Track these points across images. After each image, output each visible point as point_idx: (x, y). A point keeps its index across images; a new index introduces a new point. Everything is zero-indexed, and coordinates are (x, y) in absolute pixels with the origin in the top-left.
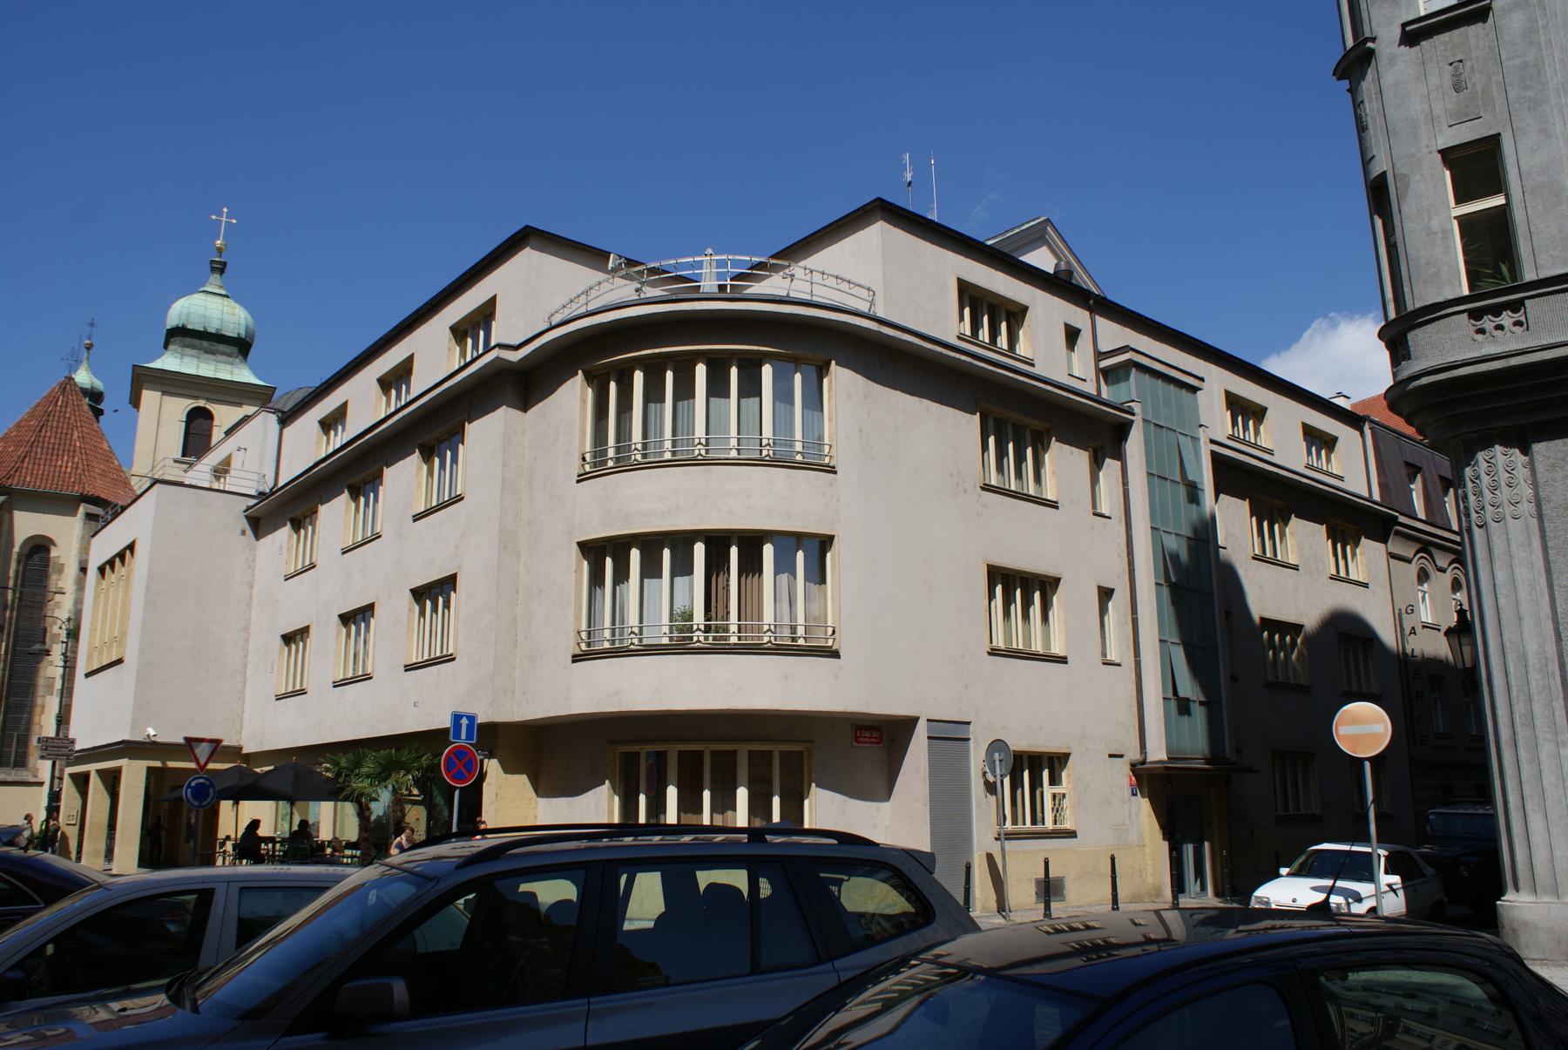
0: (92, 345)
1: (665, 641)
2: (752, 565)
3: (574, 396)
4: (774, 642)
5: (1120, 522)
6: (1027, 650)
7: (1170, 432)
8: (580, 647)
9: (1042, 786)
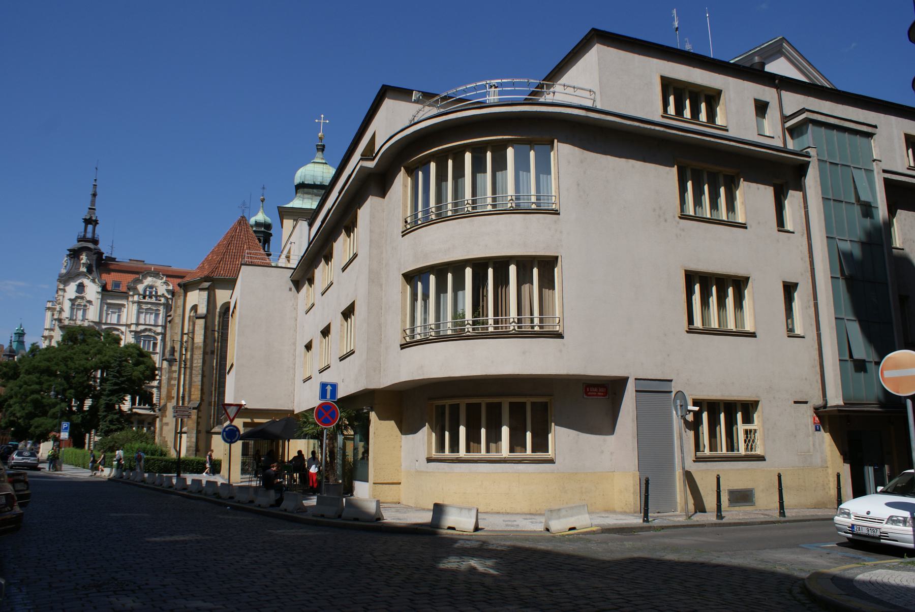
0: (264, 199)
1: (449, 332)
2: (502, 281)
3: (401, 183)
4: (517, 330)
5: (803, 235)
6: (722, 328)
7: (844, 167)
8: (405, 340)
9: (737, 424)
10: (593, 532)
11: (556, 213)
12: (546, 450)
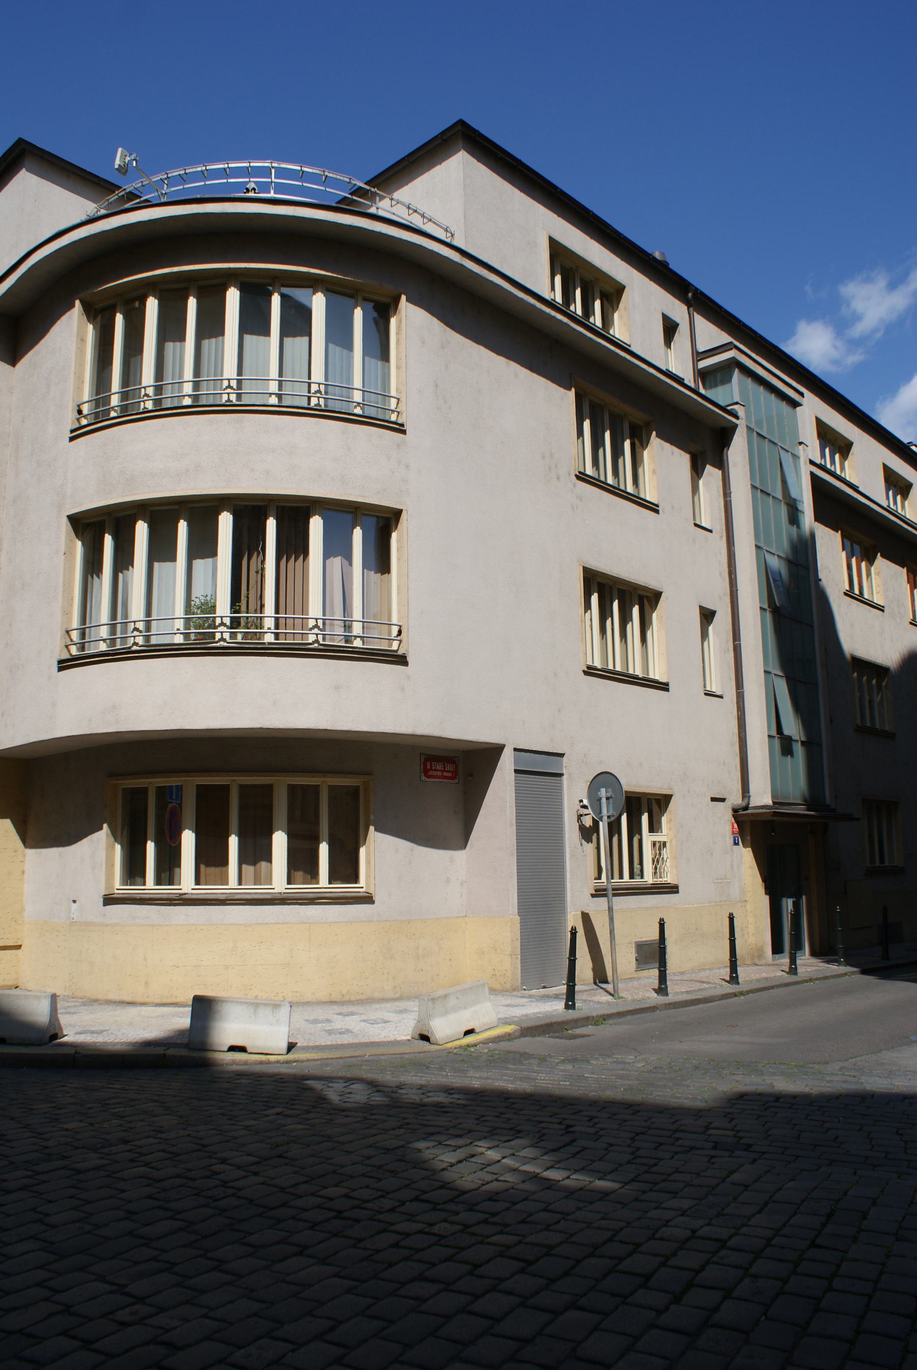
1: (179, 639)
4: (321, 642)
5: (721, 537)
8: (69, 651)
9: (640, 833)
10: (507, 1037)
11: (400, 429)
12: (355, 878)
